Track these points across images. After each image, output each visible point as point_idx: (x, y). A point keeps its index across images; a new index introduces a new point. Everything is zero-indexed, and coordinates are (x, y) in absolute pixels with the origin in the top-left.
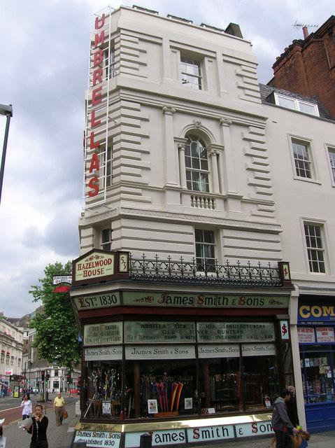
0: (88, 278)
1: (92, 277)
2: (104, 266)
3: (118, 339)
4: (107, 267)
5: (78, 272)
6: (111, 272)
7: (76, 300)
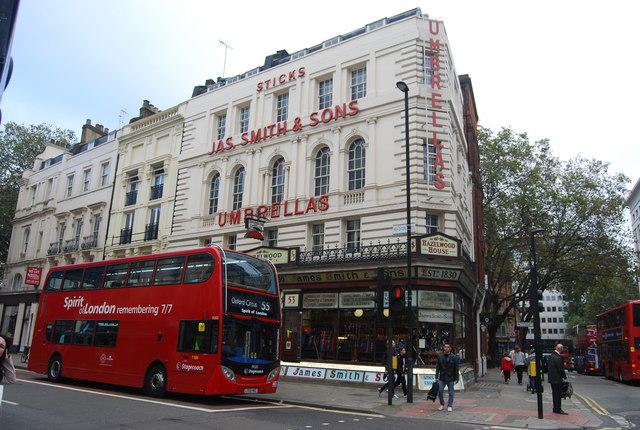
3: (450, 305)
4: (451, 249)
5: (422, 247)
6: (455, 255)
7: (420, 270)
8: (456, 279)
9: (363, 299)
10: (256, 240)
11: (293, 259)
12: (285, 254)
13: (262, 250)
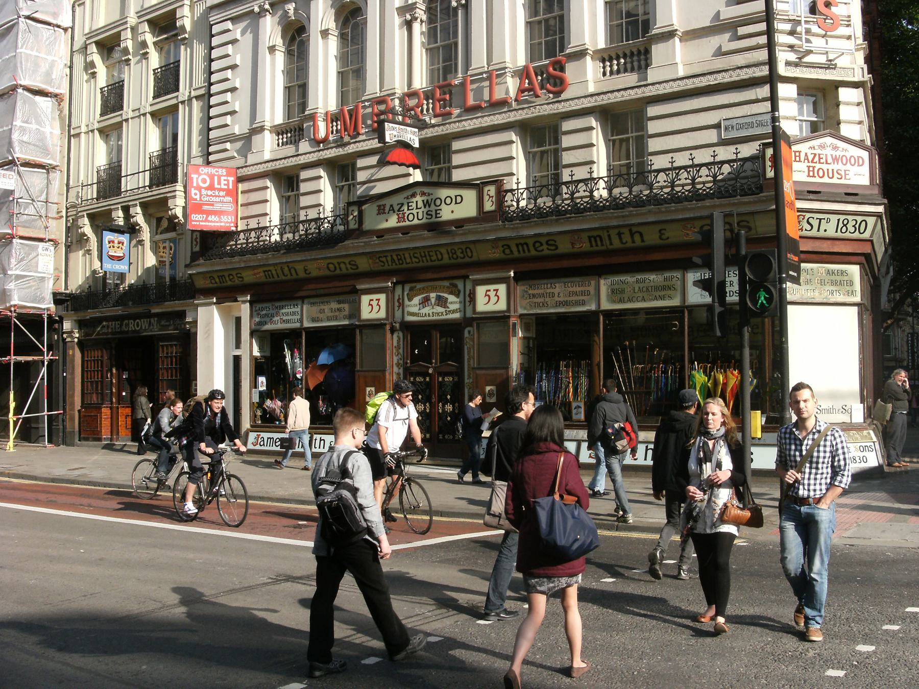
0: (817, 180)
1: (826, 180)
2: (848, 166)
3: (853, 293)
8: (867, 235)
9: (657, 288)
10: (402, 170)
11: (489, 206)
12: (470, 196)
13: (418, 190)
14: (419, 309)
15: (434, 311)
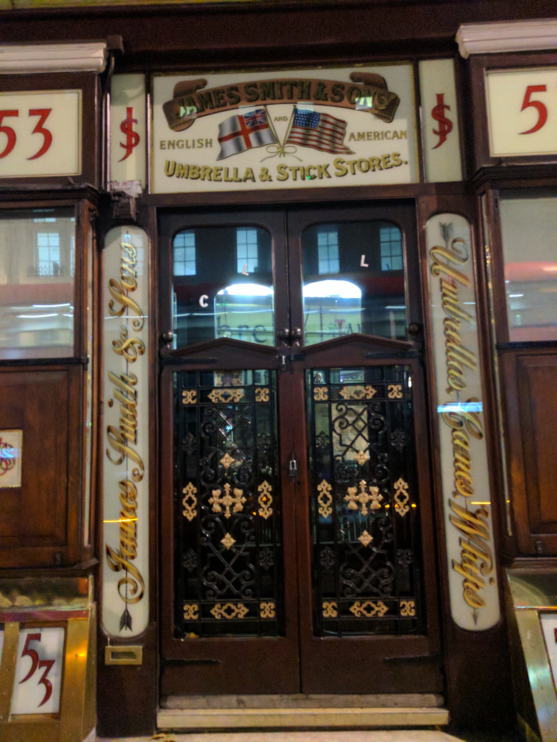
14: (222, 156)
15: (290, 161)
